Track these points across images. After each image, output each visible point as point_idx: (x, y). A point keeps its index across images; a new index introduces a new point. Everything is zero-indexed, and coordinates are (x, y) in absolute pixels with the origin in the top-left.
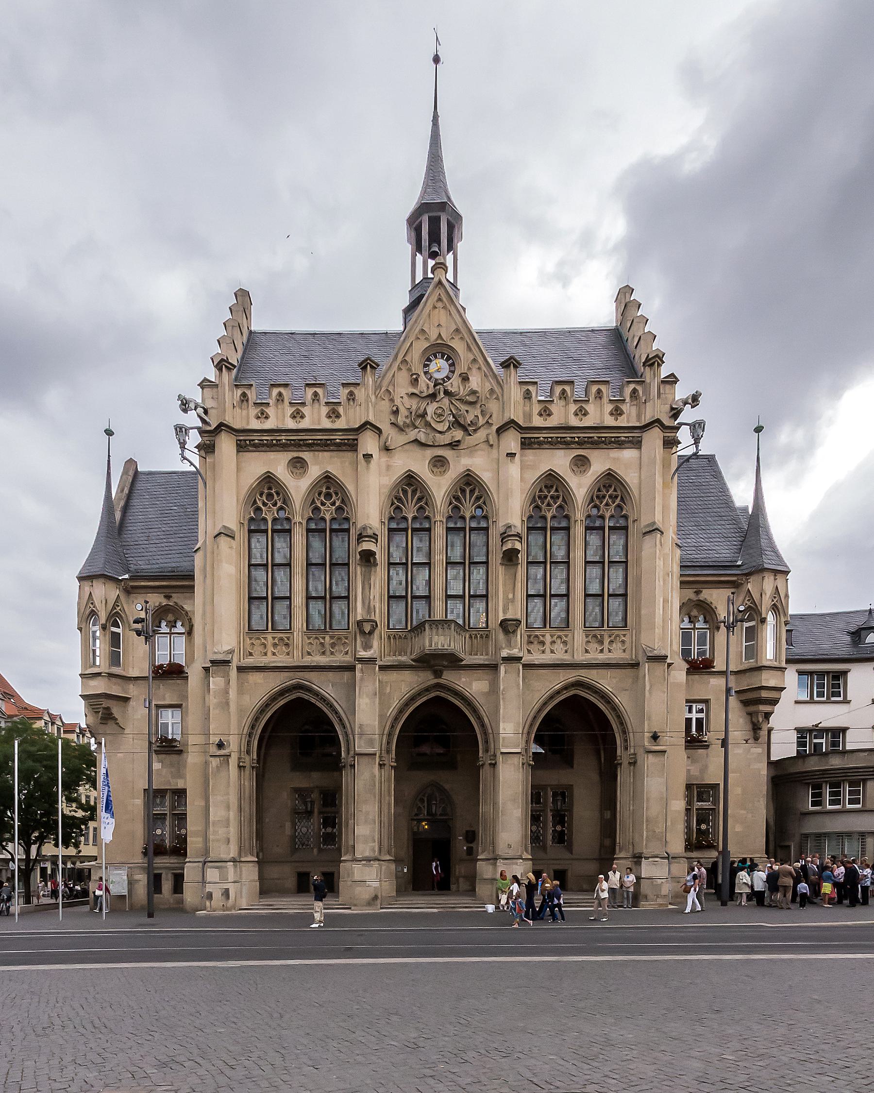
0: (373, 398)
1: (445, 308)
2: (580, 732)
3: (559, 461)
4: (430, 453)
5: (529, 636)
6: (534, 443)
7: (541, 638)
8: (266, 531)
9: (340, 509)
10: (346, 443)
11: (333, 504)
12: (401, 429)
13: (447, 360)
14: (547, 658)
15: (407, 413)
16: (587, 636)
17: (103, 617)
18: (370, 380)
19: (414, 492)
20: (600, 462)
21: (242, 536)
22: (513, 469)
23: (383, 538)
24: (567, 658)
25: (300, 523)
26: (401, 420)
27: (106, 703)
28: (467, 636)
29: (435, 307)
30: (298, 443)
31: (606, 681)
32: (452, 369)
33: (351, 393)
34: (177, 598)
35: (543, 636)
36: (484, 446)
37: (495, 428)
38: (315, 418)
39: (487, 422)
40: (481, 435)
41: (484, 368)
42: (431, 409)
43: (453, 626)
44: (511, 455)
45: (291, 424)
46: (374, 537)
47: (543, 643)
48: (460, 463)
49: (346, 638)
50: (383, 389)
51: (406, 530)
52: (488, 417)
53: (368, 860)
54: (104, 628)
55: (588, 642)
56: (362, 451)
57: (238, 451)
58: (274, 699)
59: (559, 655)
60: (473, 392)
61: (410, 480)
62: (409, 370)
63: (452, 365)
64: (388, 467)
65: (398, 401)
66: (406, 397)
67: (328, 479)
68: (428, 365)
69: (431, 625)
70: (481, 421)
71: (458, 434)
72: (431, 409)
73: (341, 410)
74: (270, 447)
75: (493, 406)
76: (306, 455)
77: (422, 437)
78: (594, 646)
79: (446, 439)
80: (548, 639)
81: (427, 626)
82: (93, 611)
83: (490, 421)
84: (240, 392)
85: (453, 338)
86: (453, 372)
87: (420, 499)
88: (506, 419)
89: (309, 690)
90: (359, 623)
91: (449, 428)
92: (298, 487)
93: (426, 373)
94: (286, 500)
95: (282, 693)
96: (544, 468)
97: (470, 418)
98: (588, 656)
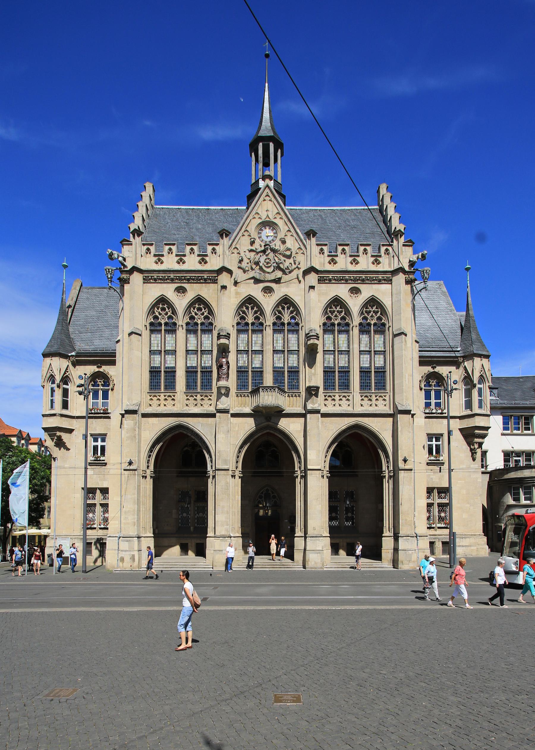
0: (227, 252)
1: (270, 200)
3: (342, 291)
4: (262, 285)
5: (325, 396)
6: (327, 280)
7: (333, 397)
8: (161, 330)
9: (206, 318)
10: (211, 277)
11: (203, 314)
12: (245, 271)
13: (272, 230)
14: (337, 410)
15: (249, 261)
16: (361, 396)
17: (58, 379)
18: (226, 241)
19: (252, 308)
20: (367, 291)
21: (146, 333)
22: (313, 294)
24: (350, 410)
25: (182, 326)
26: (244, 265)
27: (58, 434)
28: (287, 395)
29: (265, 200)
30: (181, 278)
31: (372, 424)
32: (276, 235)
33: (214, 249)
34: (105, 369)
35: (334, 396)
36: (296, 281)
37: (302, 270)
38: (192, 263)
39: (297, 267)
40: (294, 274)
41: (295, 235)
42: (263, 259)
43: (277, 389)
45: (177, 267)
47: (334, 400)
48: (280, 291)
49: (211, 396)
50: (233, 247)
51: (247, 331)
52: (297, 263)
54: (59, 386)
55: (362, 400)
57: (144, 283)
60: (289, 249)
61: (250, 301)
62: (249, 236)
63: (276, 233)
64: (237, 293)
65: (242, 254)
66: (247, 251)
68: (261, 233)
69: (263, 390)
70: (294, 266)
73: (207, 259)
74: (164, 280)
75: (300, 258)
76: (186, 286)
78: (366, 402)
79: (272, 277)
80: (337, 398)
81: (261, 390)
82: (52, 375)
83: (299, 266)
84: (146, 247)
85: (275, 218)
86: (276, 237)
87: (256, 312)
88: (309, 266)
91: (274, 271)
93: (259, 238)
94: (174, 312)
96: (332, 295)
97: (287, 264)
98: (362, 408)
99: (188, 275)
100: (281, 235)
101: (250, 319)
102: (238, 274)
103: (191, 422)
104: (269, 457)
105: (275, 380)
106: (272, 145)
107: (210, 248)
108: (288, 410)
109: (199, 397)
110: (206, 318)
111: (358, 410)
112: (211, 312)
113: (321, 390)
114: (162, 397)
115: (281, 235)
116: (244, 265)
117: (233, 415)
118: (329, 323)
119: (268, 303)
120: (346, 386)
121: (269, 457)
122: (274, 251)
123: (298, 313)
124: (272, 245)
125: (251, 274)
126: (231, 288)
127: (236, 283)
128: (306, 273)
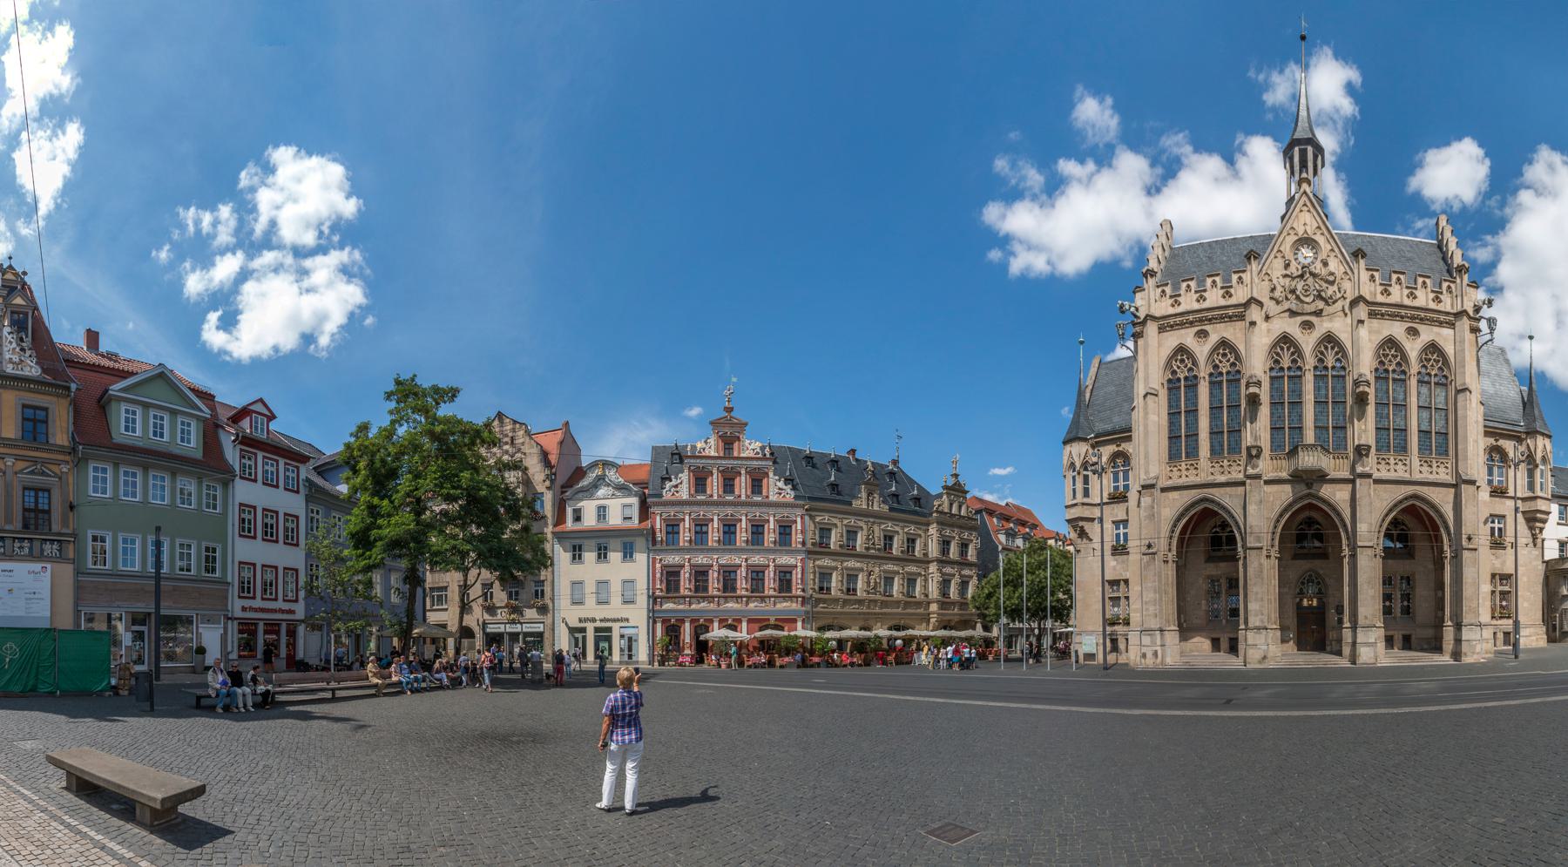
2: (1417, 532)
4: (1299, 319)
9: (1233, 364)
10: (1237, 314)
12: (1278, 303)
14: (1392, 475)
18: (1255, 266)
22: (1363, 332)
23: (1266, 385)
24: (1407, 476)
26: (1277, 294)
30: (1200, 320)
38: (1214, 298)
40: (1339, 305)
42: (1299, 287)
44: (1361, 322)
46: (1259, 384)
48: (1323, 326)
53: (1258, 628)
56: (1248, 319)
58: (1187, 510)
59: (1401, 474)
67: (1224, 343)
71: (1321, 304)
72: (1299, 287)
75: (1347, 285)
76: (1207, 328)
77: (1294, 308)
79: (1312, 308)
80: (1392, 461)
89: (1213, 501)
90: (1248, 449)
92: (1202, 350)
95: (1193, 505)
96: (1386, 333)
97: (1330, 292)
99: (1209, 314)
100: (1322, 256)
101: (1286, 363)
102: (1271, 307)
103: (1216, 494)
104: (1311, 533)
105: (1317, 438)
106: (1310, 149)
107: (1235, 277)
108: (1333, 475)
109: (1226, 463)
110: (1233, 364)
111: (1417, 477)
112: (1238, 357)
113: (1373, 450)
114: (1184, 466)
115: (1322, 256)
116: (1277, 294)
117: (1266, 482)
118: (1381, 369)
119: (1308, 342)
120: (1403, 449)
121: (1311, 533)
122: (1313, 275)
123: (1345, 355)
124: (1312, 268)
125: (1286, 305)
126: (1262, 325)
127: (1267, 318)
128: (1354, 303)
